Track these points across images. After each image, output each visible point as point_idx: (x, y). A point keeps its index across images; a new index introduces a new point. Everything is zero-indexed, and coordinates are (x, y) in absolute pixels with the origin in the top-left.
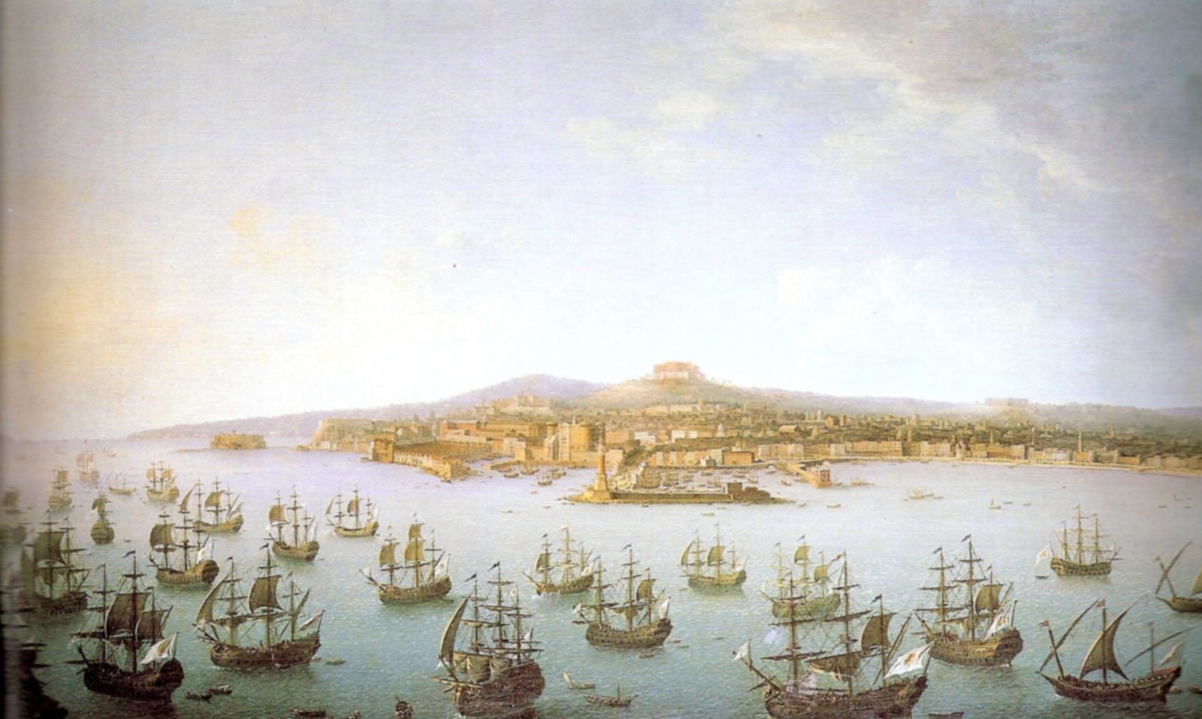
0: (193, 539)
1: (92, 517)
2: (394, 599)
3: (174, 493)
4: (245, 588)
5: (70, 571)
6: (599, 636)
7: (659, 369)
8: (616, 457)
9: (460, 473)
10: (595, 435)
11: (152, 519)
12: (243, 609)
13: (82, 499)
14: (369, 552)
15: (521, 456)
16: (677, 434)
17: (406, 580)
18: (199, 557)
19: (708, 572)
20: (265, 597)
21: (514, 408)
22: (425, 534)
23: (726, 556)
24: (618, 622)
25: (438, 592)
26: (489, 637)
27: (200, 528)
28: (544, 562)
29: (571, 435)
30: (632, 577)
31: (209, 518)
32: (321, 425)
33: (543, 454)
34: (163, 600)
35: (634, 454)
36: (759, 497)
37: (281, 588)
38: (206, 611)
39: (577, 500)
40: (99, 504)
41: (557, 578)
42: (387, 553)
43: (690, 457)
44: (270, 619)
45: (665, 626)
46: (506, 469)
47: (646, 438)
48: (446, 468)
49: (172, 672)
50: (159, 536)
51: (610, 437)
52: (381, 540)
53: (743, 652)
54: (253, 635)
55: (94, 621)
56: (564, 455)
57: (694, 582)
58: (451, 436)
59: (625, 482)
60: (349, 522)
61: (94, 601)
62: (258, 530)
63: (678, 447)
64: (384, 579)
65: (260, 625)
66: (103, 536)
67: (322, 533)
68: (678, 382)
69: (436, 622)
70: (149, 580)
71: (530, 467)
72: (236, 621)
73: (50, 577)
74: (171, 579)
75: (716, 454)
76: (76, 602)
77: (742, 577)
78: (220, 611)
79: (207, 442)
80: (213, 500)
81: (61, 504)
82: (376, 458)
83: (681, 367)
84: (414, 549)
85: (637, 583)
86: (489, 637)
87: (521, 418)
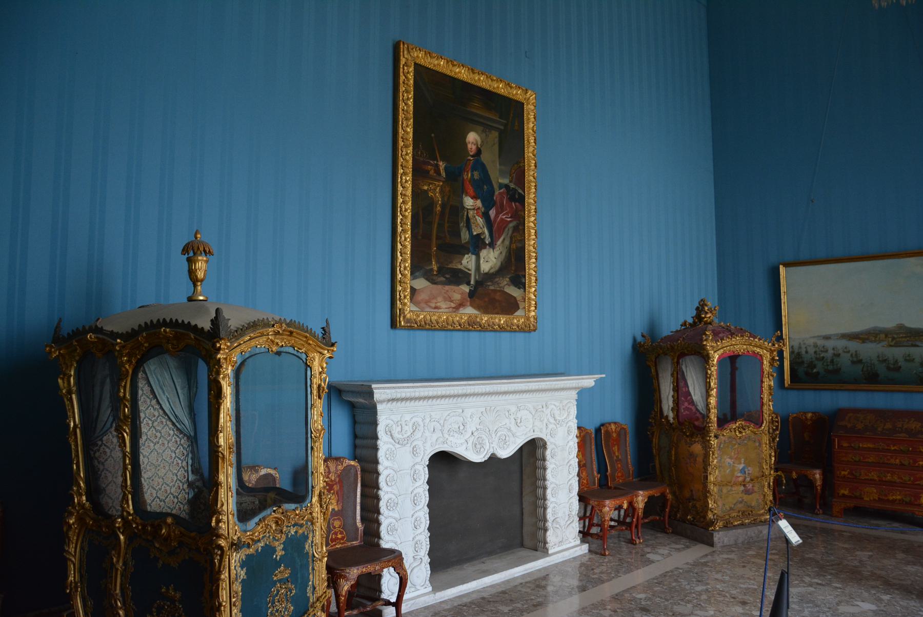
0: (820, 353)
1: (805, 349)
2: (853, 362)
3: (817, 346)
4: (829, 360)
5: (801, 358)
6: (888, 368)
7: (897, 325)
8: (890, 339)
9: (864, 342)
10: (886, 336)
11: (814, 350)
12: (829, 363)
13: (803, 347)
14: (849, 355)
15: (873, 339)
16: (901, 335)
17: (855, 359)
18: (822, 355)
19: (908, 358)
20: (832, 361)
21: (872, 332)
22: (858, 352)
23: (911, 355)
24: (892, 366)
25: (860, 361)
26: (869, 368)
27: (822, 351)
28: (878, 357)
29: (883, 336)
30: (894, 359)
31: (823, 349)
32: (840, 335)
33: (877, 339)
34: (816, 362)
35: (893, 339)
36: (918, 346)
37: (835, 361)
38: (823, 364)
39: (884, 346)
40: (806, 348)
41: (881, 359)
42: (852, 355)
43: (903, 339)
44: (833, 365)
45: (900, 367)
46: (871, 342)
47: (895, 336)
48: (861, 341)
49: (818, 373)
50: (815, 352)
51: (889, 336)
52: (851, 353)
53: (915, 372)
54: (830, 368)
55: (806, 365)
56: (881, 339)
57: (906, 360)
58: (861, 336)
59: (892, 344)
60: (845, 350)
61: (806, 362)
62: (831, 352)
63: (902, 337)
64: (851, 359)
65: (832, 367)
66: (807, 352)
67: (841, 352)
68: (901, 327)
69: (860, 367)
70: (814, 359)
71: (875, 341)
72: (828, 365)
73: (799, 358)
74: (817, 359)
75: (908, 339)
76: (803, 362)
77: (914, 359)
78: (825, 364)
79: (822, 338)
80: (823, 347)
81: (800, 348)
82: (849, 340)
83: (901, 324)
84: (856, 355)
85: (895, 360)
86: (869, 368)
87: (874, 333)
